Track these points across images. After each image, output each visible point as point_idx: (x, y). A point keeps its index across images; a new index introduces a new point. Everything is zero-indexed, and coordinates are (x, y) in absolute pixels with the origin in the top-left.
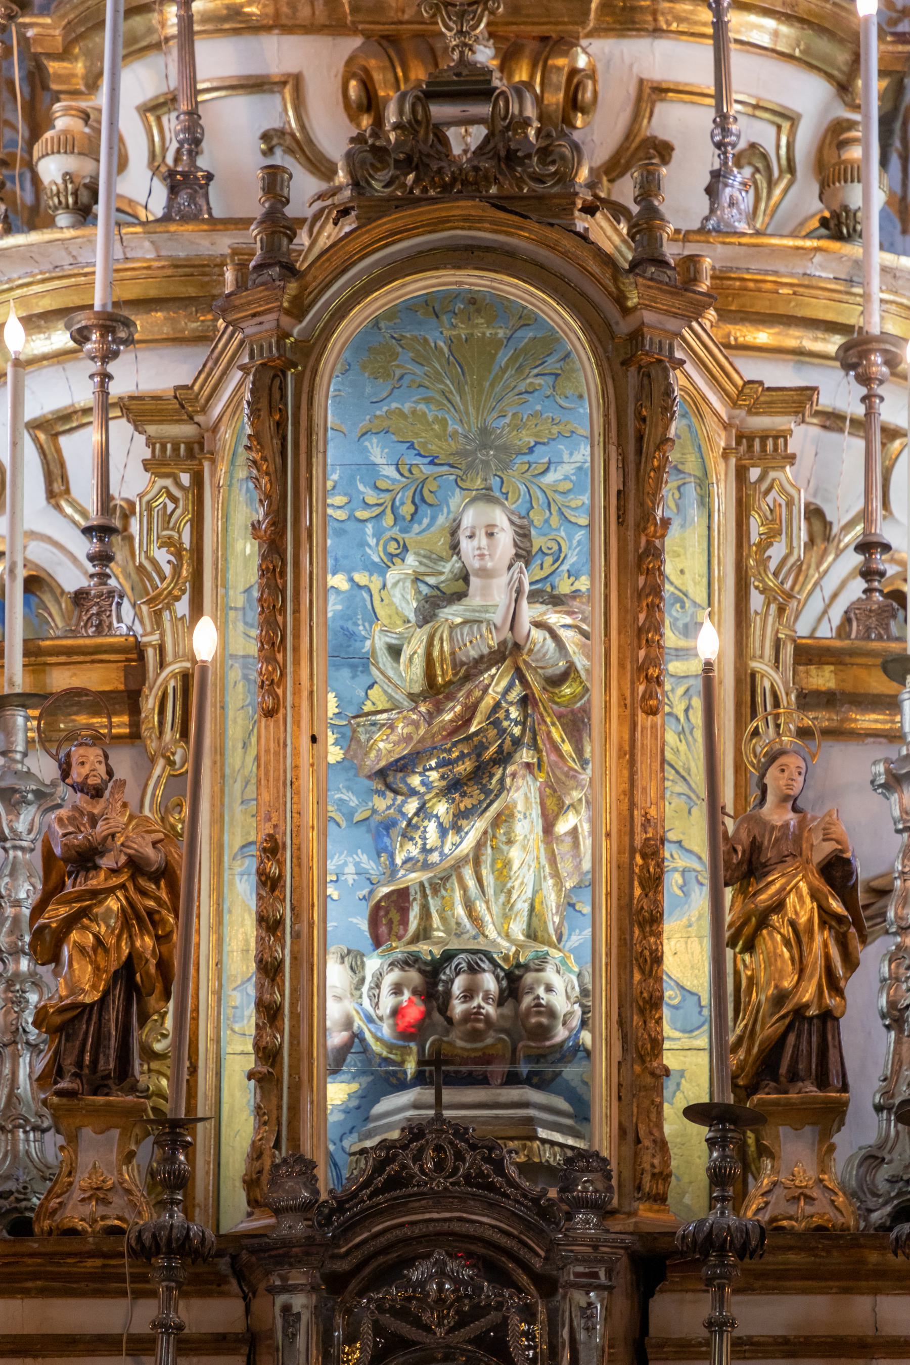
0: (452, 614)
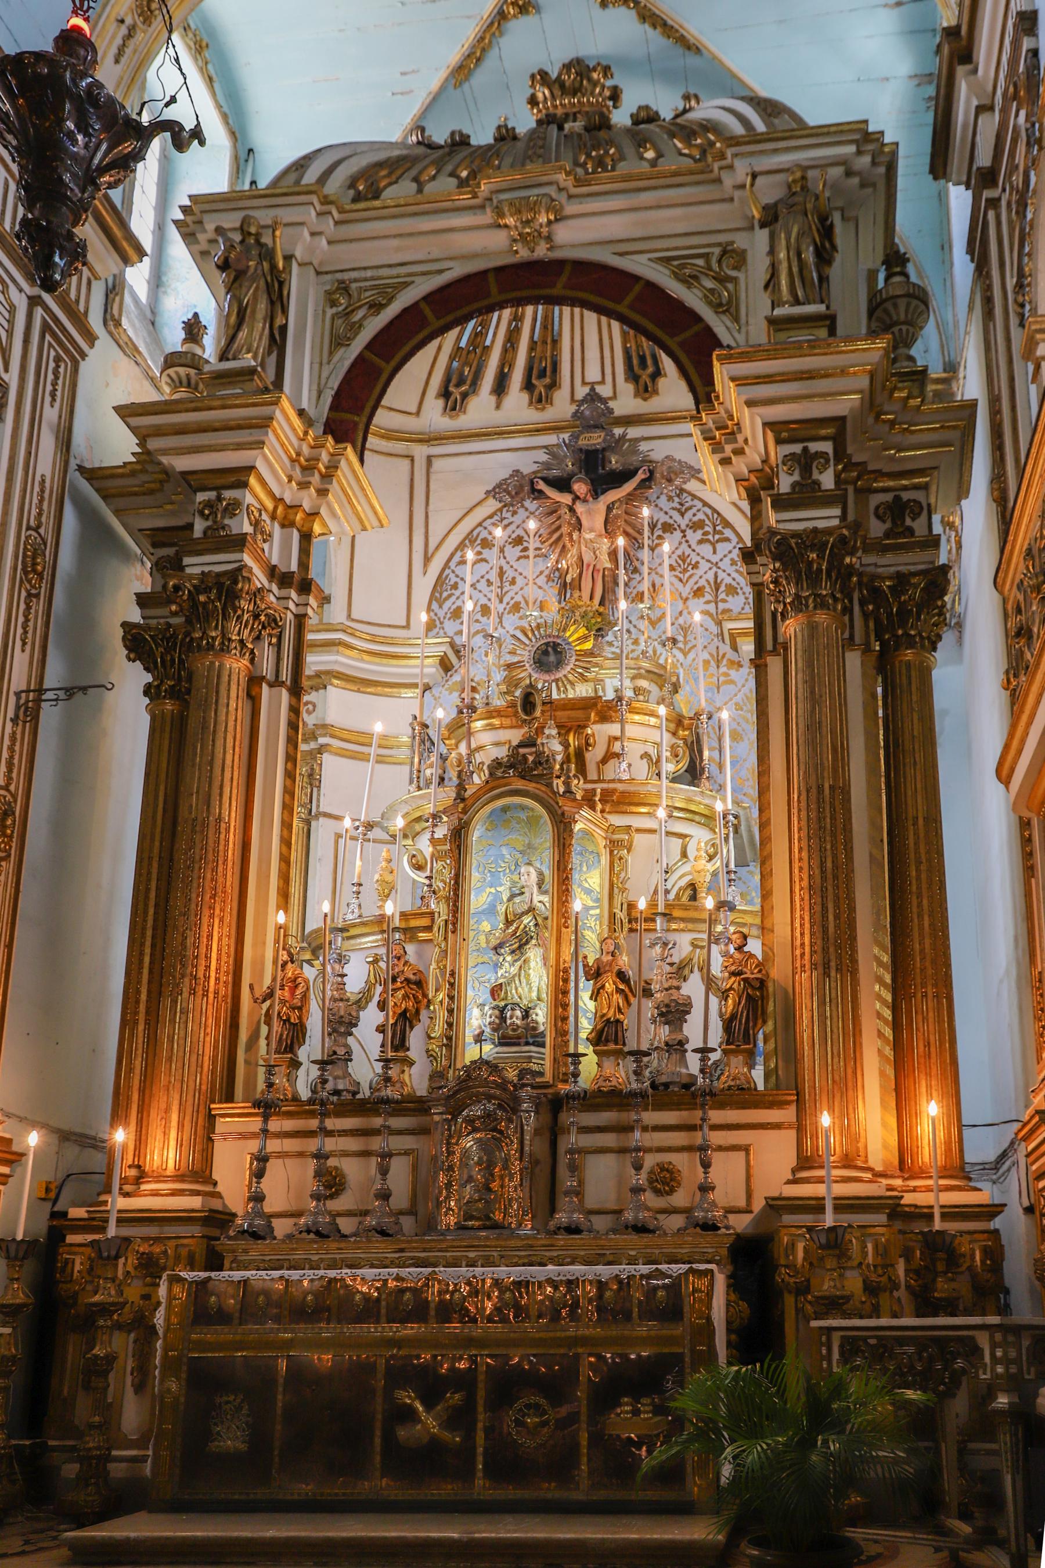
0: (517, 900)
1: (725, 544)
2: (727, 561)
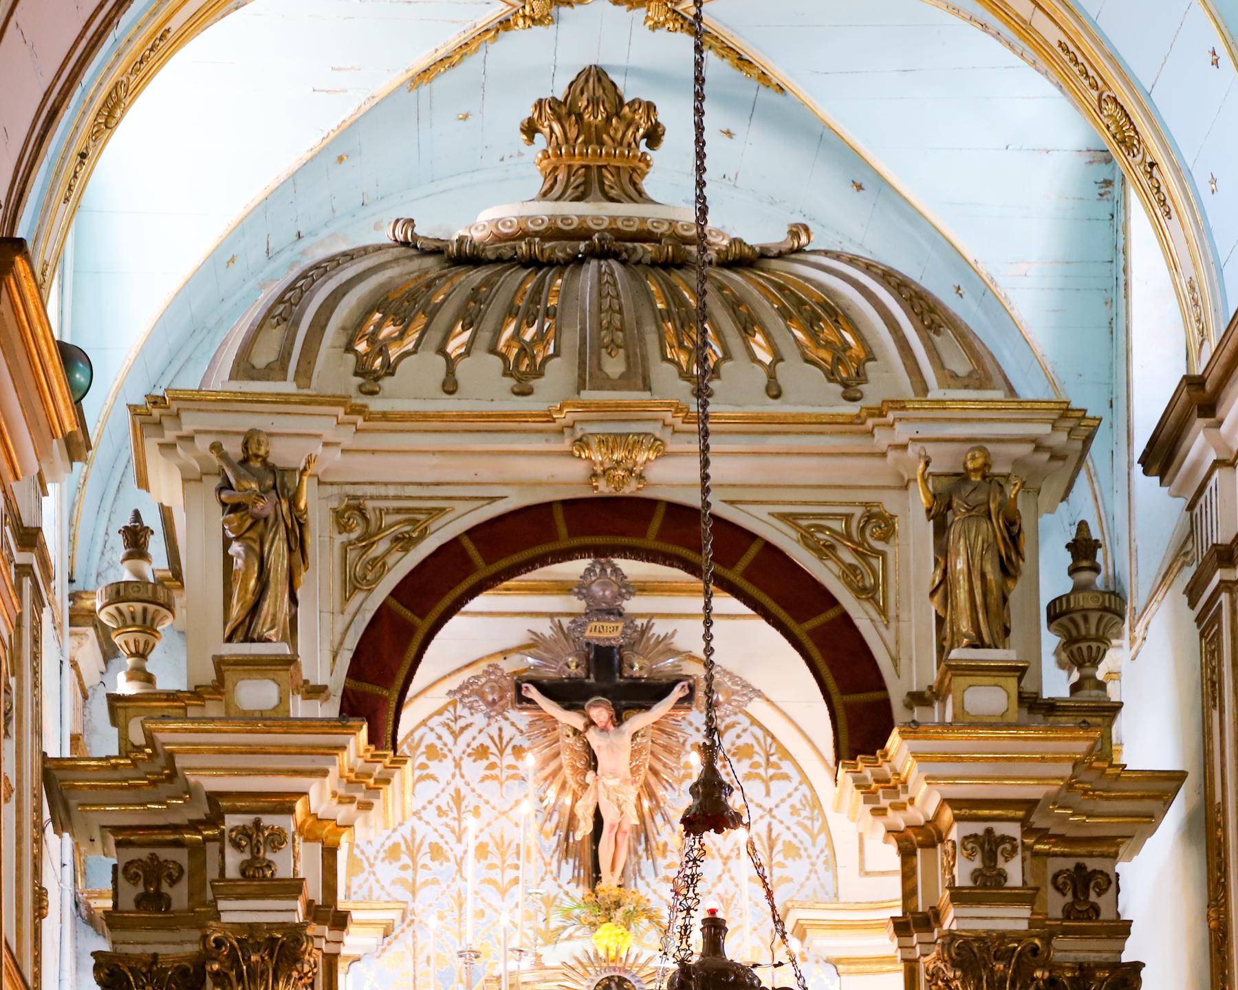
1: (782, 783)
2: (785, 808)
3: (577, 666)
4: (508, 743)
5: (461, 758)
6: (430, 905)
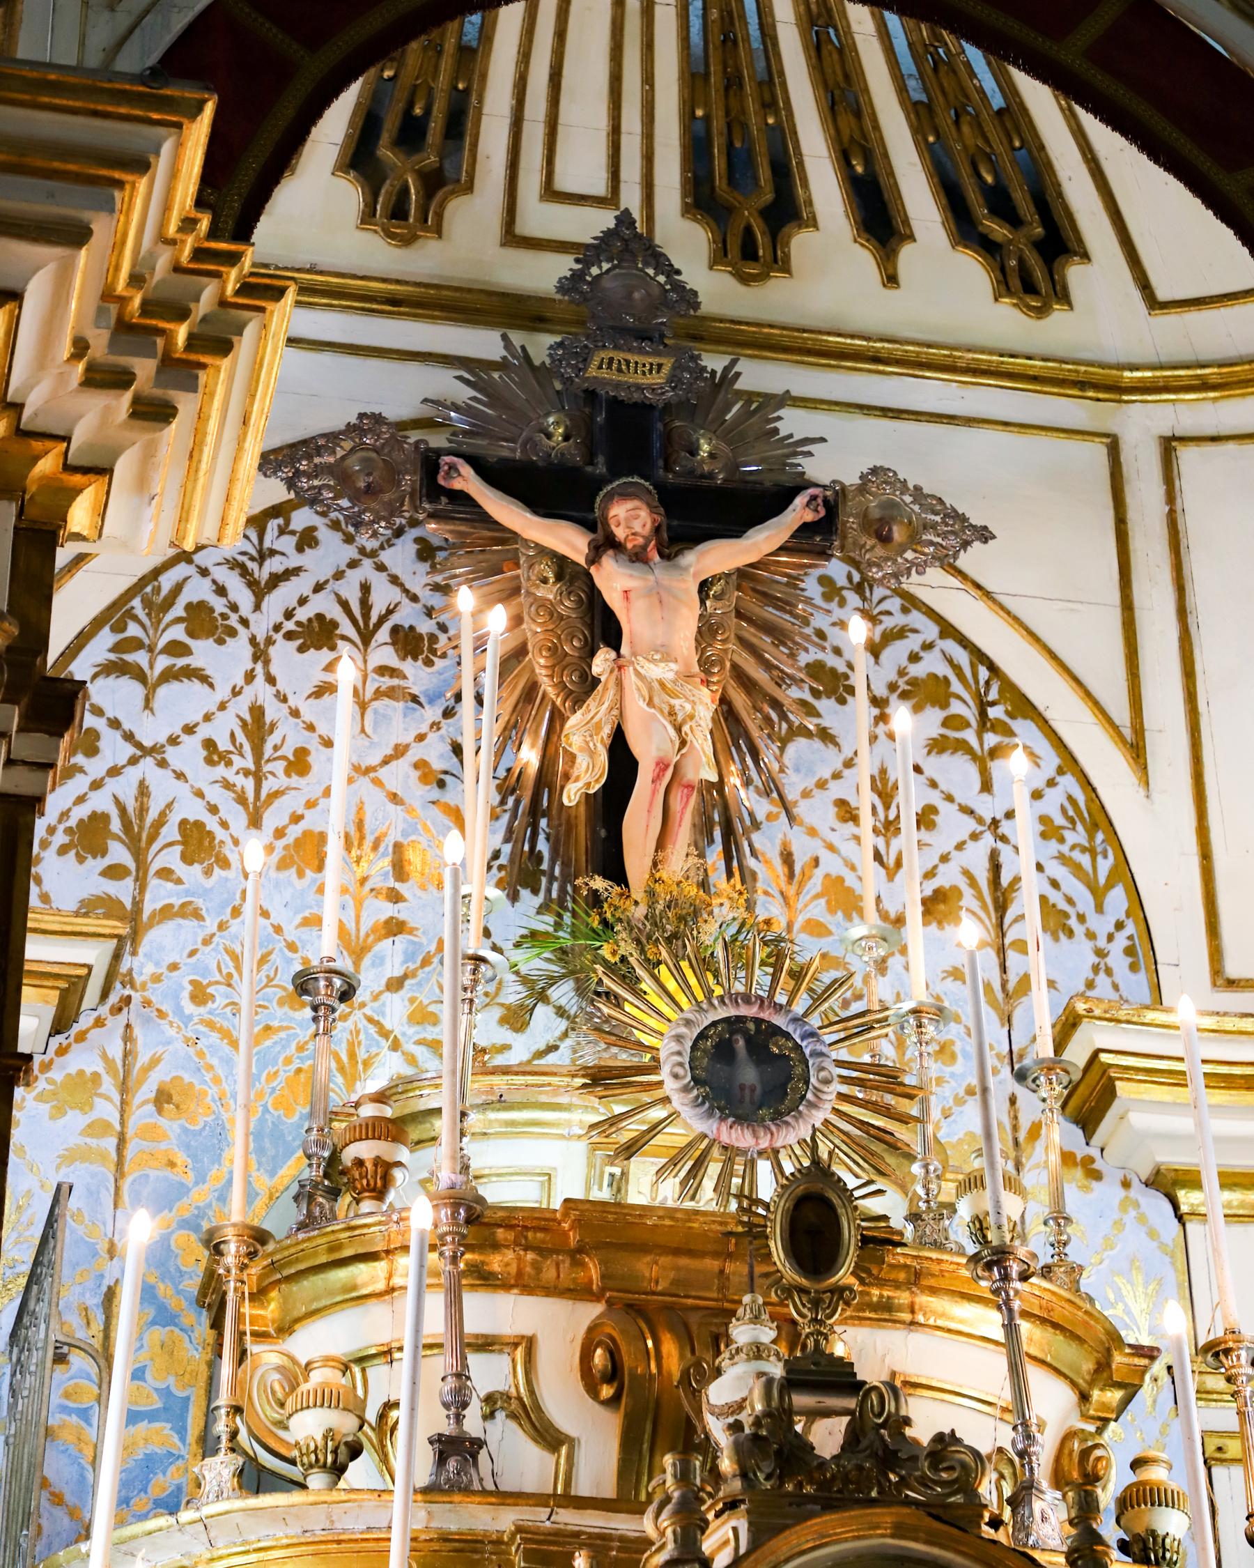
3: (566, 438)
4: (382, 620)
5: (270, 641)
6: (174, 967)
